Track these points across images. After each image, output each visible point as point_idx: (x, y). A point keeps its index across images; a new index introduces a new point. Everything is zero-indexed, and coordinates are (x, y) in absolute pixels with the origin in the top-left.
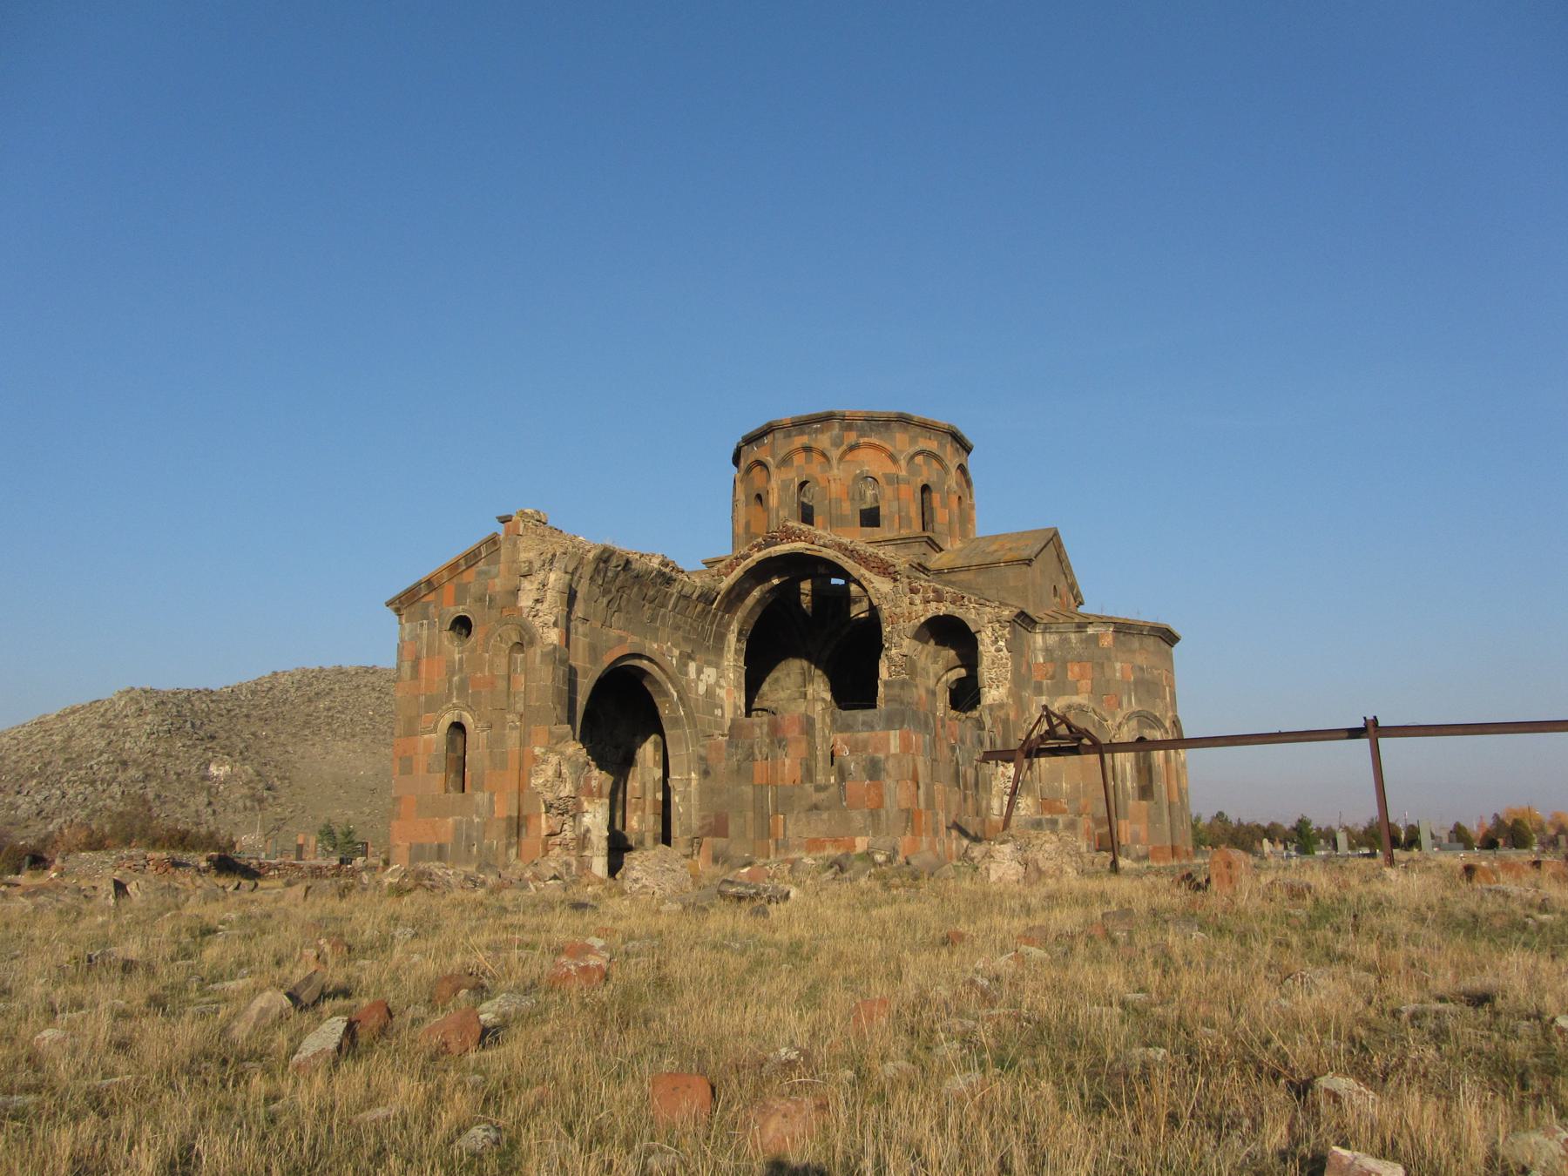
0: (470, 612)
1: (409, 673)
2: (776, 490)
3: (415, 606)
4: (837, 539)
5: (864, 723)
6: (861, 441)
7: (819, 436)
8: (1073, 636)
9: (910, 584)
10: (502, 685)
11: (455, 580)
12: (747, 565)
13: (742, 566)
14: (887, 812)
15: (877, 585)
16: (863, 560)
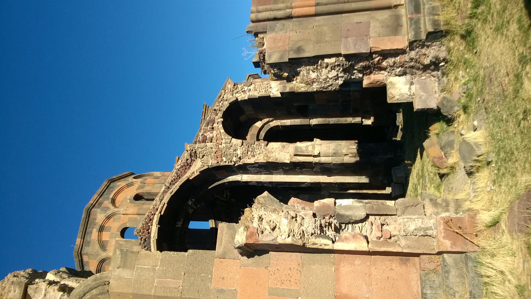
6: (111, 196)
7: (97, 221)
9: (200, 142)
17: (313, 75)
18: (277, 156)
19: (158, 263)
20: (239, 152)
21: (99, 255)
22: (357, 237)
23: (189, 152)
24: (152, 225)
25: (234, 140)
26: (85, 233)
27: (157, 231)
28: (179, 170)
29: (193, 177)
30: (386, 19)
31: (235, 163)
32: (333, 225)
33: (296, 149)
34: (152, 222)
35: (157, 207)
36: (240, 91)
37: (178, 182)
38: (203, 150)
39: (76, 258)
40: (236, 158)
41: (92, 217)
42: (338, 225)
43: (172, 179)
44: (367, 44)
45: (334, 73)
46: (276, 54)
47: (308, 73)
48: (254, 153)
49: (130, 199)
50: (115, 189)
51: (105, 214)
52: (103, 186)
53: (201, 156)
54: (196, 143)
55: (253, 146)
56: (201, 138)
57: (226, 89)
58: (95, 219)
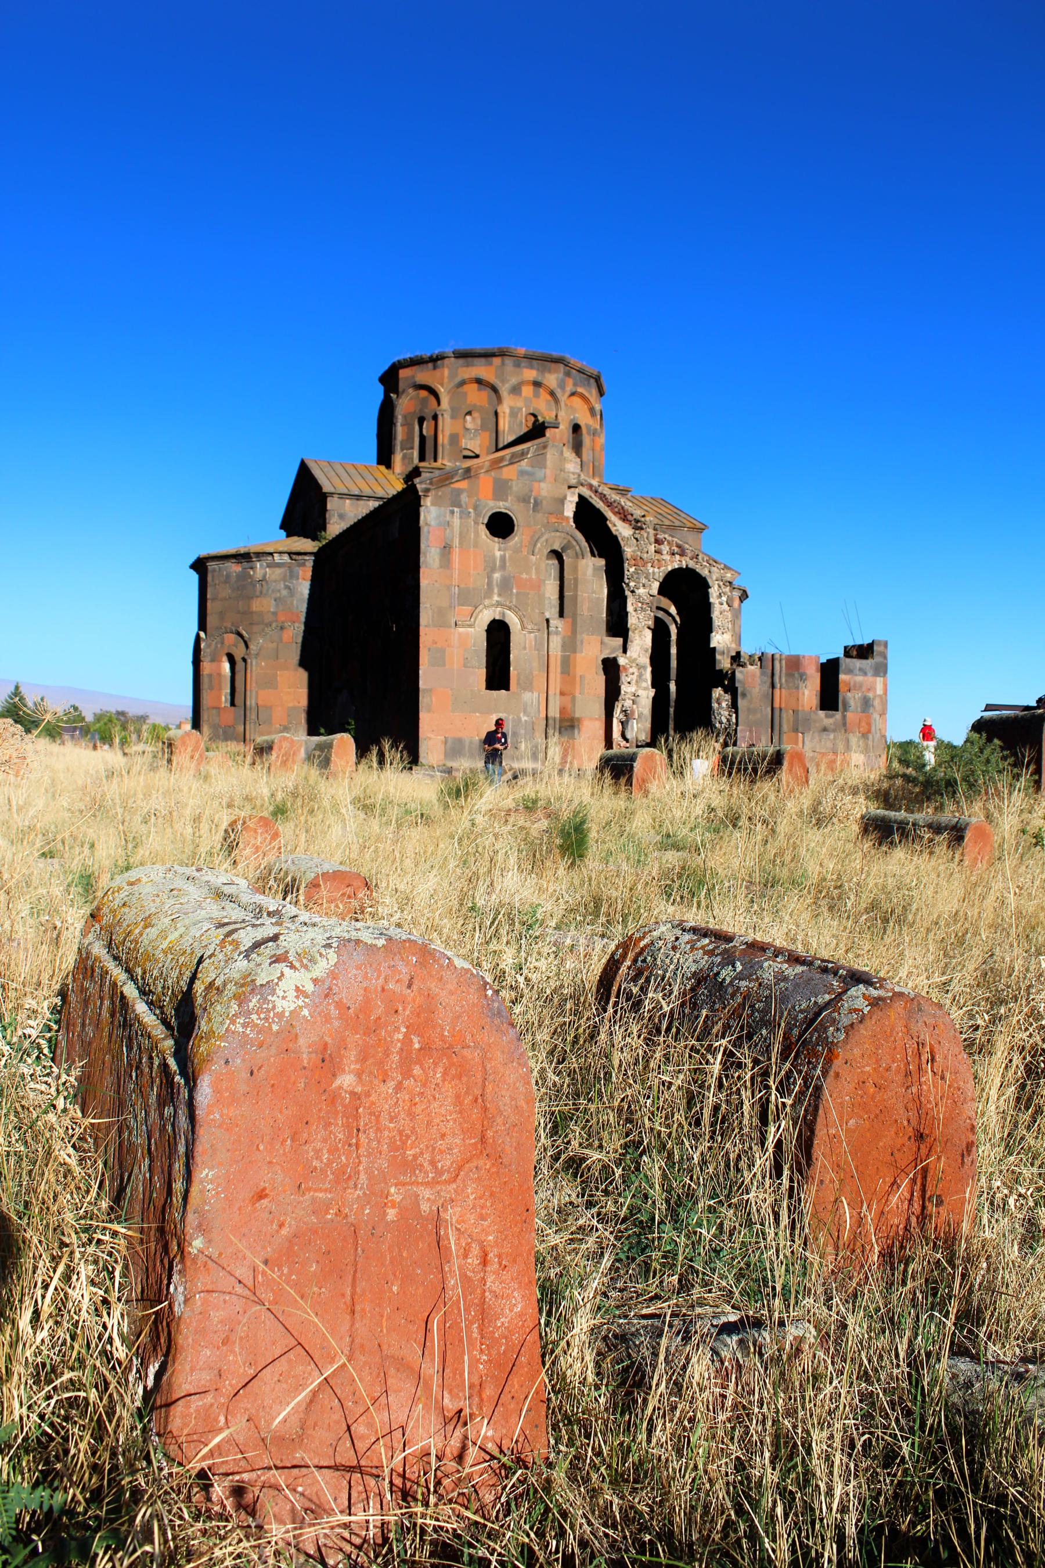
1: (437, 560)
5: (860, 669)
6: (580, 390)
7: (547, 375)
9: (656, 535)
11: (493, 473)
15: (621, 530)
16: (609, 505)
17: (724, 704)
18: (636, 642)
20: (641, 591)
21: (503, 385)
25: (656, 585)
26: (530, 358)
29: (610, 525)
31: (628, 585)
33: (644, 668)
39: (499, 349)
41: (553, 365)
45: (724, 720)
56: (660, 536)
58: (550, 372)
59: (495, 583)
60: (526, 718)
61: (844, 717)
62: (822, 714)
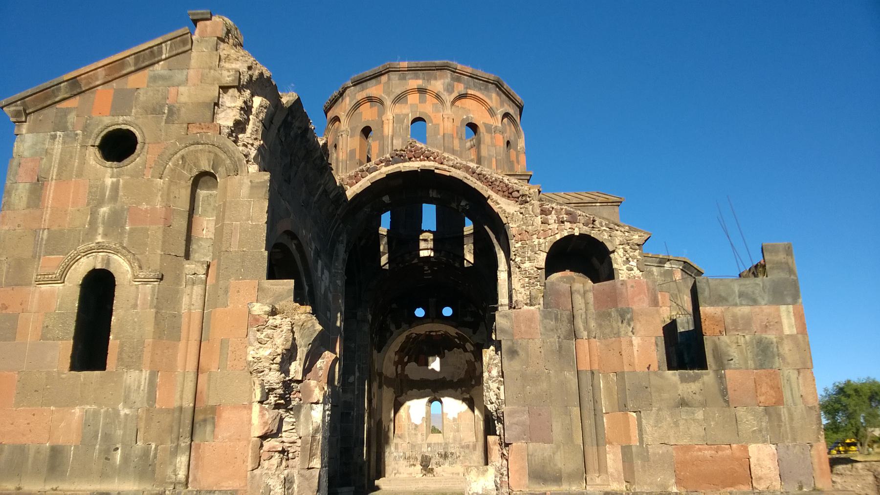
0: (136, 126)
1: (25, 199)
2: (391, 121)
3: (46, 111)
4: (464, 163)
5: (741, 295)
6: (470, 92)
7: (433, 82)
8: (655, 269)
9: (541, 205)
10: (180, 224)
11: (114, 84)
12: (375, 177)
13: (367, 178)
14: (789, 410)
15: (504, 207)
16: (491, 184)
19: (255, 222)
20: (527, 265)
22: (265, 426)
23: (527, 193)
24: (421, 160)
25: (544, 256)
26: (414, 70)
27: (412, 169)
28: (501, 182)
30: (555, 465)
32: (282, 401)
34: (425, 160)
35: (445, 162)
36: (627, 255)
37: (481, 185)
38: (531, 212)
39: (383, 67)
40: (519, 262)
41: (438, 73)
42: (291, 406)
43: (487, 176)
44: (518, 439)
46: (509, 324)
47: (496, 365)
48: (527, 286)
49: (468, 118)
50: (483, 94)
51: (442, 90)
52: (486, 75)
53: (522, 211)
54: (540, 200)
55: (537, 285)
56: (547, 206)
57: (632, 233)
58: (436, 79)
59: (100, 220)
60: (127, 411)
61: (721, 379)
62: (673, 376)
